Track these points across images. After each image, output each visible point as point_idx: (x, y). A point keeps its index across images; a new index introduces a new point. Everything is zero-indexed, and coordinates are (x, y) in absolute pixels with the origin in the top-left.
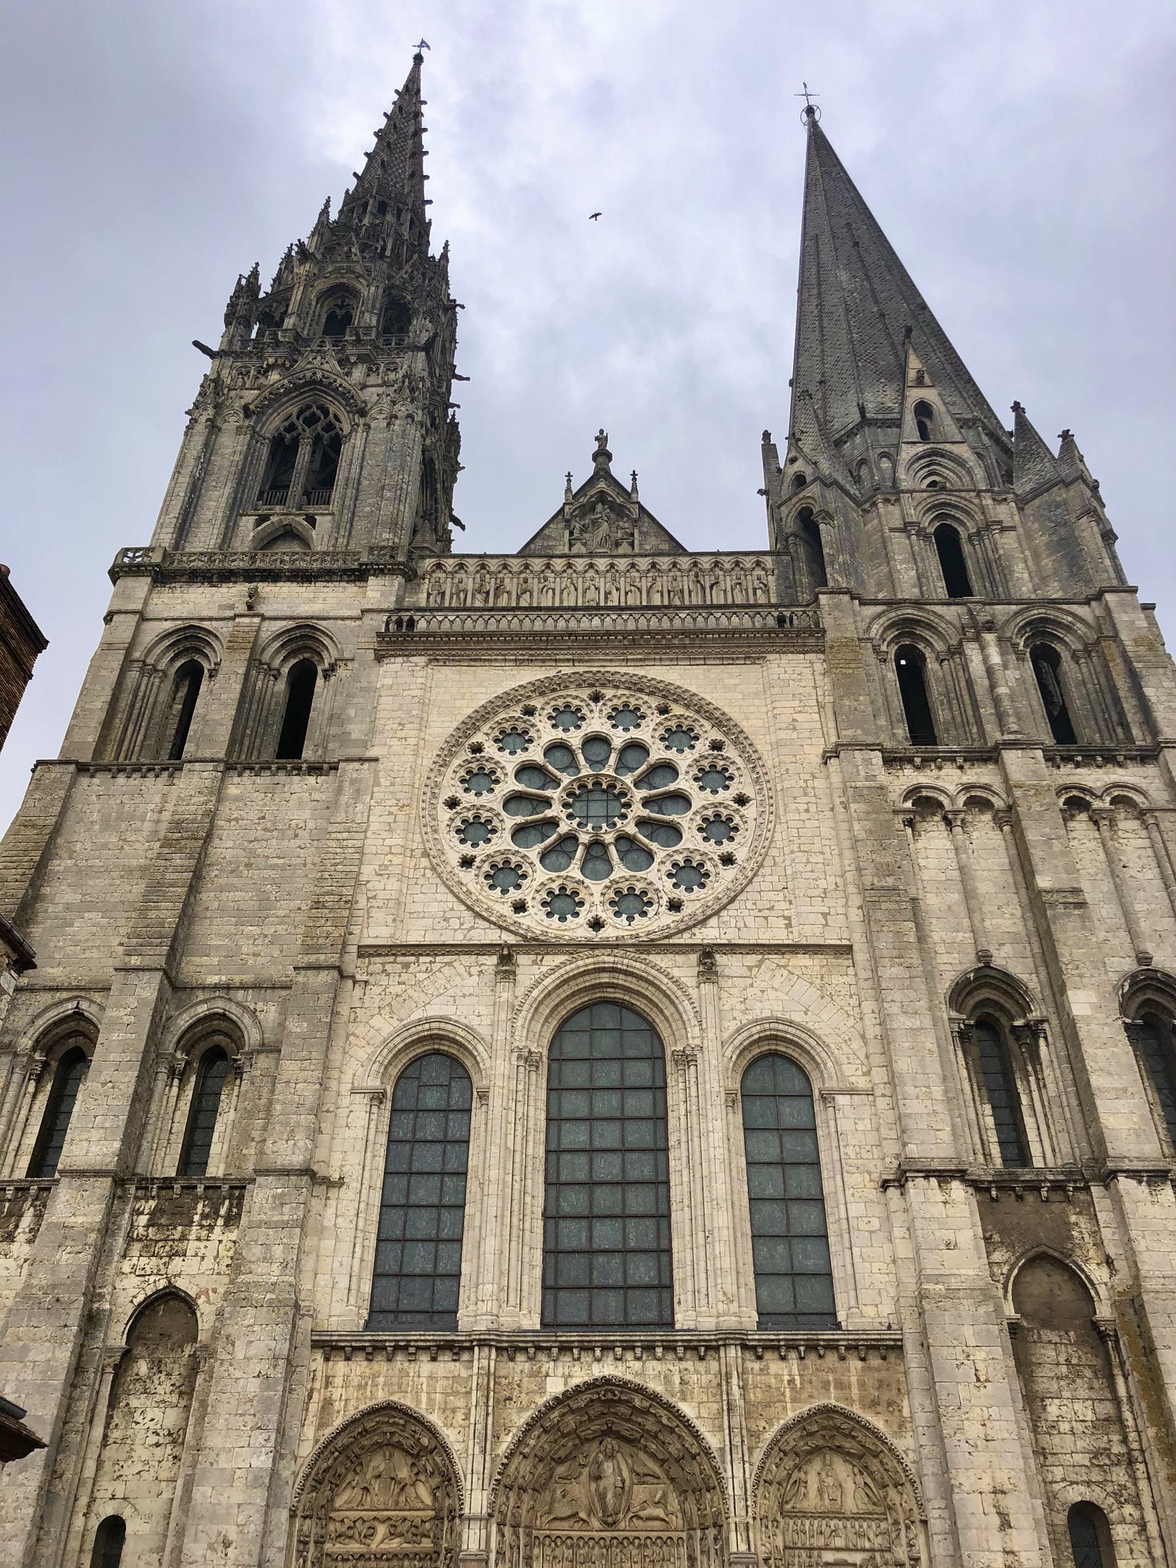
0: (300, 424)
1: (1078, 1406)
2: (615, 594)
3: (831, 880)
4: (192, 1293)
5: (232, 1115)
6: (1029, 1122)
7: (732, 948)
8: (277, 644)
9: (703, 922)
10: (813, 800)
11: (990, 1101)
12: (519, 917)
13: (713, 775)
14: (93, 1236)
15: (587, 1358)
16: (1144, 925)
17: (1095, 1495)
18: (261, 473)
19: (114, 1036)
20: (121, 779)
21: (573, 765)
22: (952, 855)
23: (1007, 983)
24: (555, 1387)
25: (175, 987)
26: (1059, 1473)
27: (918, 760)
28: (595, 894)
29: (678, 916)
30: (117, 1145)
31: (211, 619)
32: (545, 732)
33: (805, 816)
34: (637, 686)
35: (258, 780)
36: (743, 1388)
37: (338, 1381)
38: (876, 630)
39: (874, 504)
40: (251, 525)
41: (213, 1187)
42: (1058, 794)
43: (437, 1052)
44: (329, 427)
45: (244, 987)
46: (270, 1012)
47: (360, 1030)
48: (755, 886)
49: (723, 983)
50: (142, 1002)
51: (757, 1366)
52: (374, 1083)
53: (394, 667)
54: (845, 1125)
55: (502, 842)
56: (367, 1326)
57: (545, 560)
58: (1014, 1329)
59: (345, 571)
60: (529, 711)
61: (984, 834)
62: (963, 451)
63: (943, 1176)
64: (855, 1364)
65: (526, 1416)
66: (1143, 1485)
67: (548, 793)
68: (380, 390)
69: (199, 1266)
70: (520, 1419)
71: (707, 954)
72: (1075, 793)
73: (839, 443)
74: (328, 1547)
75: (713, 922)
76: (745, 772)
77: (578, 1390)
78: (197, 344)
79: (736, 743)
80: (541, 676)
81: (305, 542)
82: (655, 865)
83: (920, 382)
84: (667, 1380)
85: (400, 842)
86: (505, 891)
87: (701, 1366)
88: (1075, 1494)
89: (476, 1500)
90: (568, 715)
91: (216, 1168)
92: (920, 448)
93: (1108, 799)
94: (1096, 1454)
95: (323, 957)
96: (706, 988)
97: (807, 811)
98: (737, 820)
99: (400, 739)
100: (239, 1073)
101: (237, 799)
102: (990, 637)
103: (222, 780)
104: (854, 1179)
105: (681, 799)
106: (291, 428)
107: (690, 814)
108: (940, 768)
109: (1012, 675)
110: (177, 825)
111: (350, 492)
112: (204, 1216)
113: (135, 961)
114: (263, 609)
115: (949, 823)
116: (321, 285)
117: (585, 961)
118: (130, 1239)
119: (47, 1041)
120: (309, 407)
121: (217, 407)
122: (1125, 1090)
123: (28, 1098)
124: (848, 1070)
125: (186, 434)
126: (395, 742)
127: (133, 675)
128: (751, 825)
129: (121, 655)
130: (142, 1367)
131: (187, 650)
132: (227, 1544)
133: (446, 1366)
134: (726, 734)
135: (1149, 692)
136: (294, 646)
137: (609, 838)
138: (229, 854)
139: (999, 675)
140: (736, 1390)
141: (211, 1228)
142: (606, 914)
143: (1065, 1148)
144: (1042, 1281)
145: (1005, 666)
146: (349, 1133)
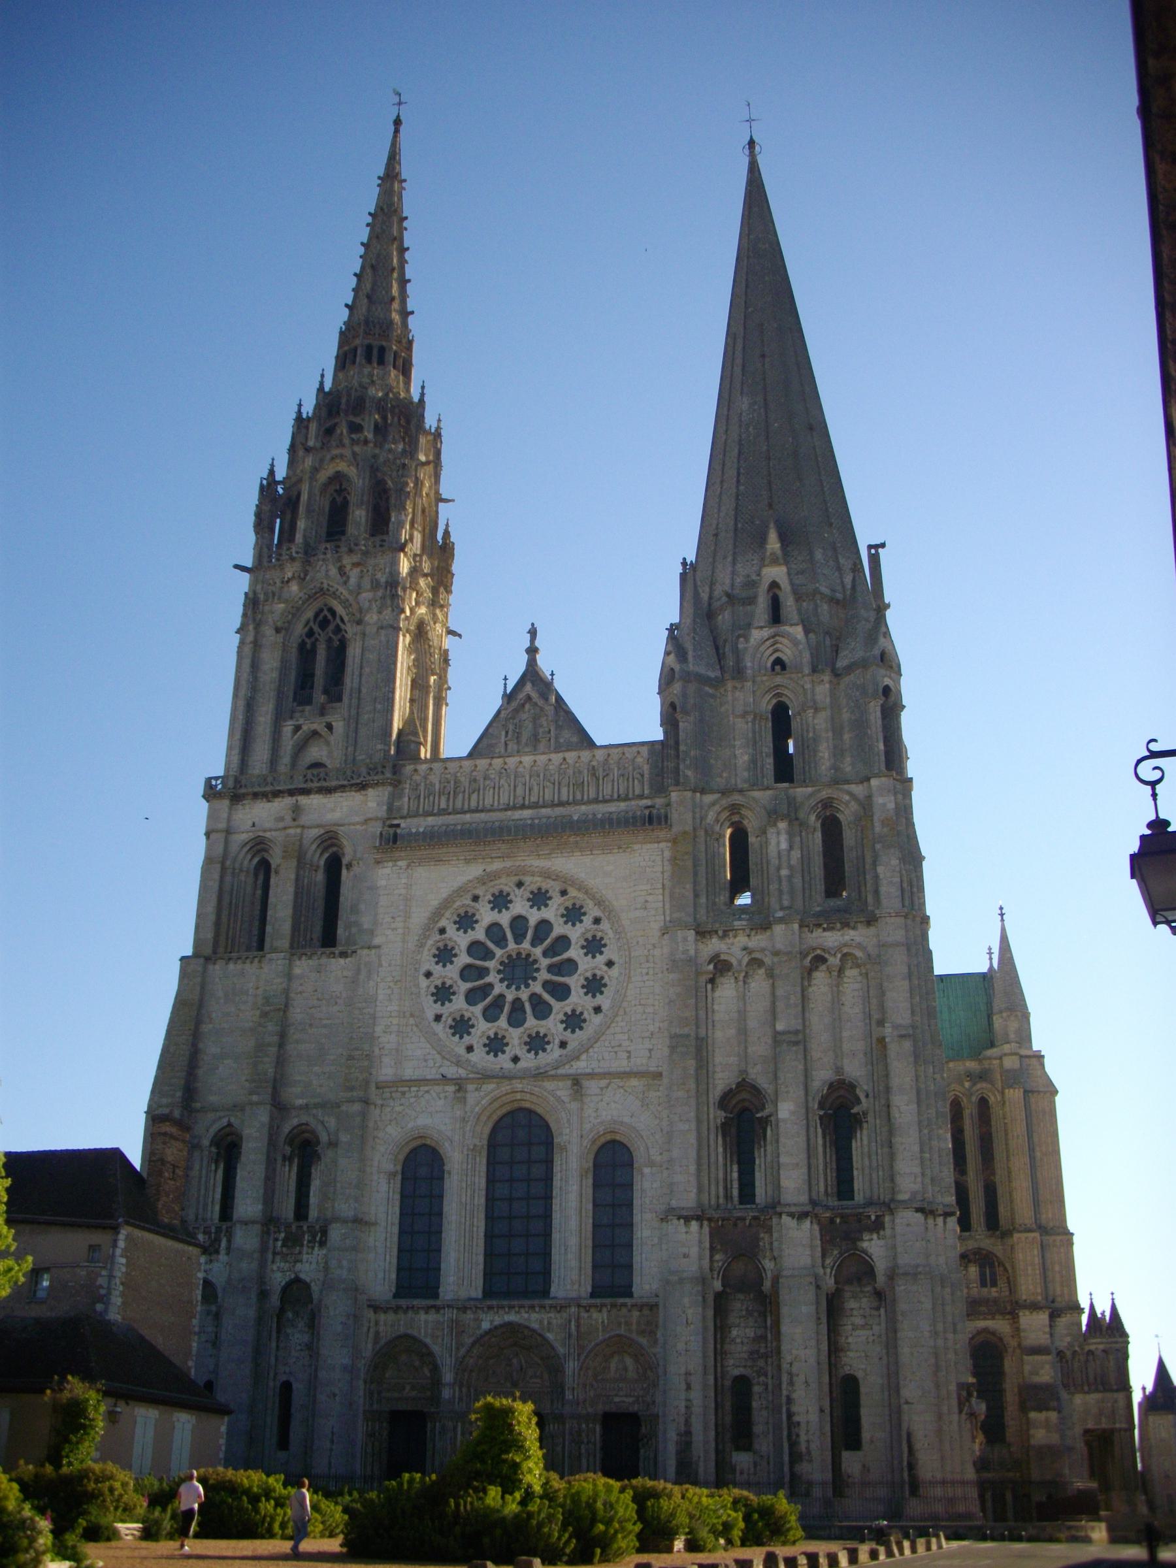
0: (316, 628)
1: (747, 1330)
2: (536, 788)
3: (657, 1025)
4: (308, 1280)
6: (757, 1174)
7: (592, 1075)
8: (314, 846)
9: (577, 1058)
10: (652, 965)
11: (739, 1163)
14: (256, 1255)
15: (501, 1312)
16: (846, 1046)
17: (747, 1372)
19: (250, 1145)
21: (501, 941)
23: (755, 1090)
24: (486, 1326)
25: (280, 1107)
26: (731, 1362)
27: (720, 933)
28: (515, 1036)
29: (564, 1052)
30: (260, 1207)
31: (270, 830)
33: (646, 978)
34: (547, 875)
35: (310, 962)
36: (578, 1326)
37: (382, 1323)
38: (711, 816)
40: (289, 735)
43: (425, 1145)
44: (338, 629)
45: (316, 1106)
46: (332, 1122)
47: (381, 1135)
48: (611, 1030)
49: (587, 1100)
51: (586, 1315)
52: (390, 1167)
54: (646, 1185)
55: (459, 1003)
56: (396, 1296)
57: (488, 761)
59: (352, 785)
60: (476, 898)
61: (759, 984)
63: (687, 1219)
64: (636, 1314)
65: (470, 1341)
66: (769, 1368)
67: (487, 964)
69: (309, 1266)
70: (468, 1341)
71: (577, 1082)
72: (819, 952)
75: (584, 1057)
78: (237, 567)
81: (328, 743)
82: (552, 1016)
83: (775, 561)
84: (541, 1322)
85: (396, 1008)
86: (461, 1037)
87: (558, 1316)
88: (736, 1372)
89: (448, 1377)
90: (500, 901)
91: (313, 1213)
92: (766, 633)
93: (839, 956)
94: (751, 1353)
95: (355, 1094)
96: (574, 1106)
97: (647, 974)
98: (606, 978)
99: (393, 929)
100: (319, 1158)
102: (782, 825)
103: (290, 964)
106: (311, 633)
107: (576, 976)
108: (735, 937)
110: (267, 1000)
111: (355, 701)
112: (309, 1242)
113: (255, 1098)
114: (304, 820)
116: (323, 476)
117: (505, 1087)
118: (275, 1254)
119: (216, 1142)
120: (321, 610)
121: (258, 625)
122: (797, 1164)
123: (212, 1175)
124: (652, 1152)
125: (238, 652)
126: (389, 932)
127: (228, 878)
129: (218, 866)
130: (290, 1315)
131: (259, 851)
132: (335, 1395)
133: (432, 1316)
135: (880, 869)
136: (325, 844)
139: (784, 859)
140: (573, 1327)
141: (313, 1248)
142: (521, 1051)
143: (770, 1193)
145: (791, 848)
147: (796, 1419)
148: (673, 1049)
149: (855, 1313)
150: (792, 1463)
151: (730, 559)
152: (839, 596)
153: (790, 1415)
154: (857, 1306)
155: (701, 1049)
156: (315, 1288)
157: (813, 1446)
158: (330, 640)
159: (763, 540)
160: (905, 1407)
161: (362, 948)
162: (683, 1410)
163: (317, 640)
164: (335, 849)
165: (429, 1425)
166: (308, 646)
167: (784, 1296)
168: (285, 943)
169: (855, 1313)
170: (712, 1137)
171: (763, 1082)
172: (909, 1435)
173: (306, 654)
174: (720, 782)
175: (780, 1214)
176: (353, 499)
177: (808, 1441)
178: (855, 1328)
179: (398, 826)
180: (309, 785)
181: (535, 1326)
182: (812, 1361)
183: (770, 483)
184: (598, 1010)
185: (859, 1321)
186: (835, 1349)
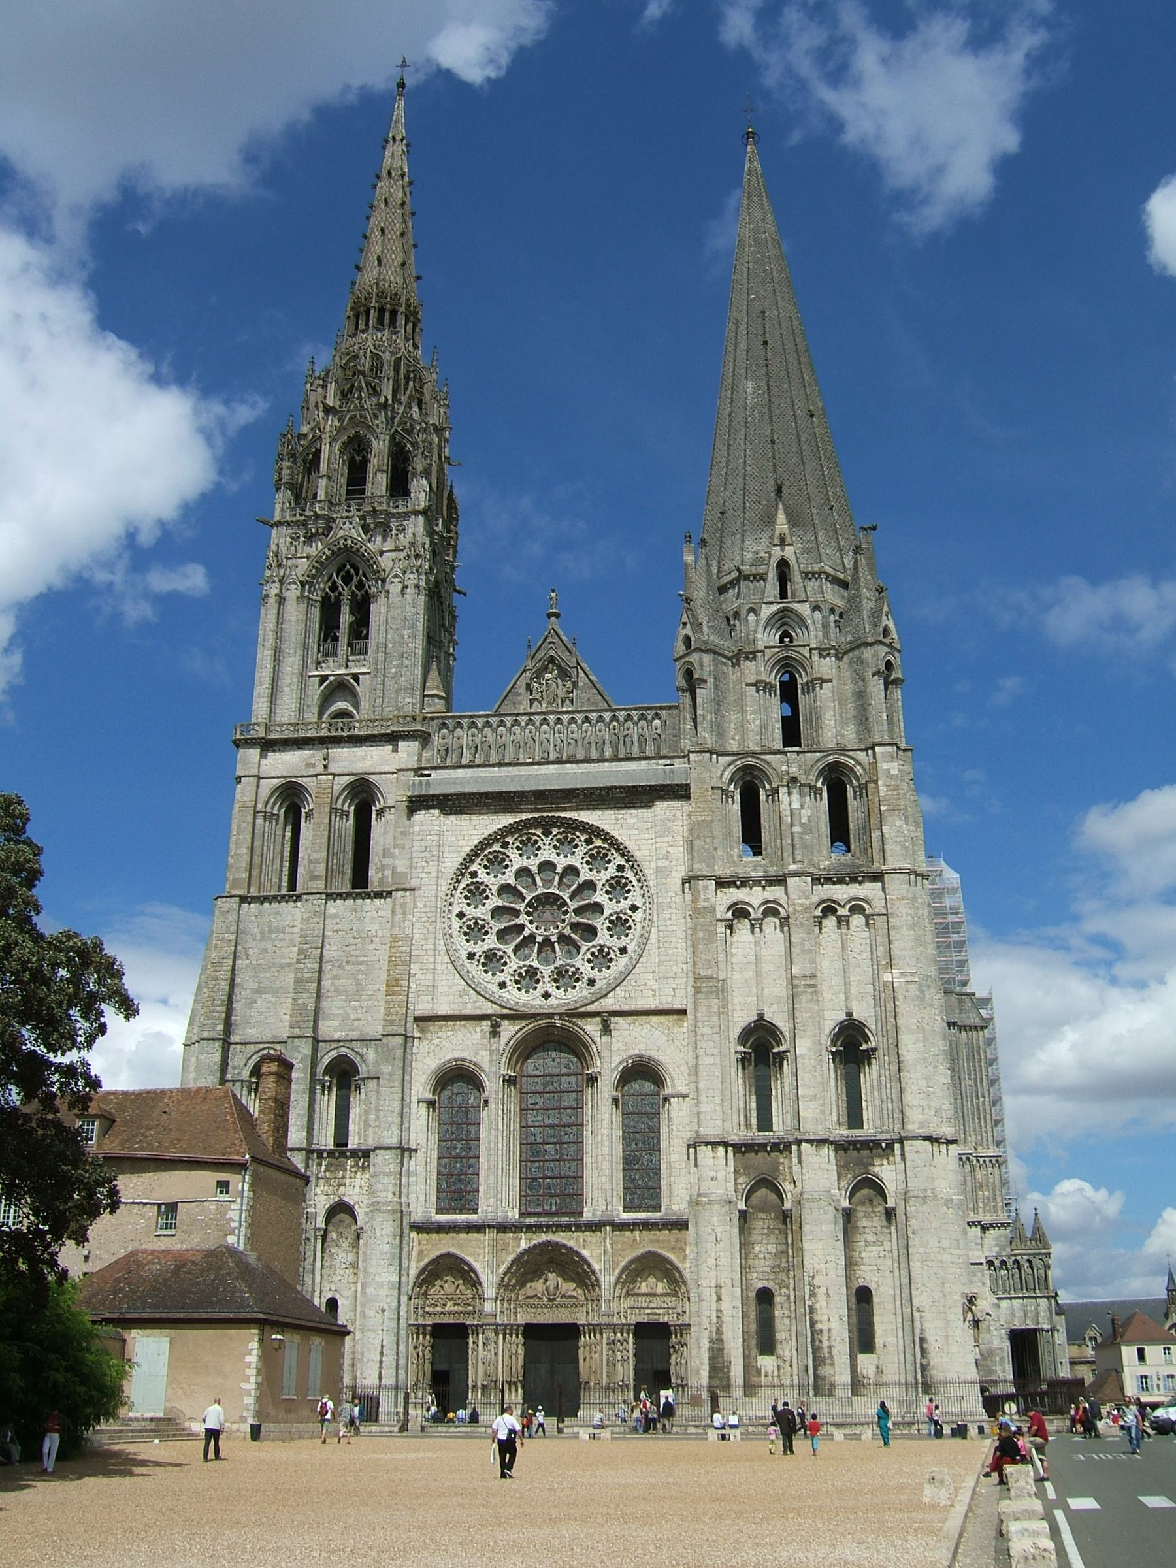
5: (358, 1110)
6: (774, 1105)
12: (502, 993)
13: (618, 886)
16: (854, 990)
17: (770, 1285)
18: (318, 619)
20: (266, 904)
22: (752, 946)
26: (755, 1275)
29: (593, 989)
32: (517, 861)
33: (669, 922)
38: (727, 774)
39: (738, 660)
41: (354, 1154)
42: (818, 905)
44: (360, 585)
46: (371, 1054)
50: (305, 1056)
52: (429, 1096)
53: (420, 816)
55: (491, 942)
58: (743, 1215)
59: (383, 735)
60: (505, 845)
62: (804, 609)
63: (714, 1145)
65: (511, 1258)
66: (792, 1281)
68: (393, 555)
73: (722, 590)
74: (427, 1309)
75: (611, 995)
76: (637, 888)
77: (535, 1246)
79: (632, 867)
80: (512, 821)
84: (577, 1240)
86: (494, 975)
88: (760, 1285)
89: (490, 1292)
90: (529, 846)
91: (353, 1143)
92: (775, 608)
98: (630, 923)
100: (358, 1088)
101: (336, 916)
104: (674, 1142)
105: (598, 908)
106: (334, 587)
109: (805, 814)
111: (381, 656)
112: (352, 1167)
113: (297, 1032)
114: (333, 768)
115: (752, 925)
118: (318, 1178)
126: (424, 875)
127: (259, 821)
128: (639, 926)
130: (334, 1235)
132: (383, 1311)
134: (627, 861)
137: (554, 939)
138: (335, 954)
139: (796, 818)
142: (552, 990)
144: (762, 1192)
145: (802, 807)
146: (418, 1123)
147: (818, 1326)
148: (697, 990)
149: (867, 1230)
150: (815, 1368)
151: (739, 536)
152: (842, 576)
153: (813, 1324)
154: (870, 1223)
155: (721, 990)
156: (360, 1212)
157: (834, 1352)
158: (353, 594)
159: (769, 520)
160: (917, 1315)
161: (397, 890)
162: (714, 1320)
163: (340, 594)
164: (364, 795)
165: (471, 1340)
166: (332, 599)
167: (807, 1217)
168: (320, 885)
169: (867, 1230)
170: (734, 1070)
171: (781, 1021)
172: (922, 1340)
173: (330, 610)
174: (733, 746)
175: (799, 1143)
176: (374, 462)
177: (830, 1347)
178: (867, 1244)
179: (429, 775)
180: (340, 733)
181: (571, 1243)
182: (832, 1273)
183: (774, 465)
184: (623, 950)
185: (871, 1238)
186: (850, 1264)
